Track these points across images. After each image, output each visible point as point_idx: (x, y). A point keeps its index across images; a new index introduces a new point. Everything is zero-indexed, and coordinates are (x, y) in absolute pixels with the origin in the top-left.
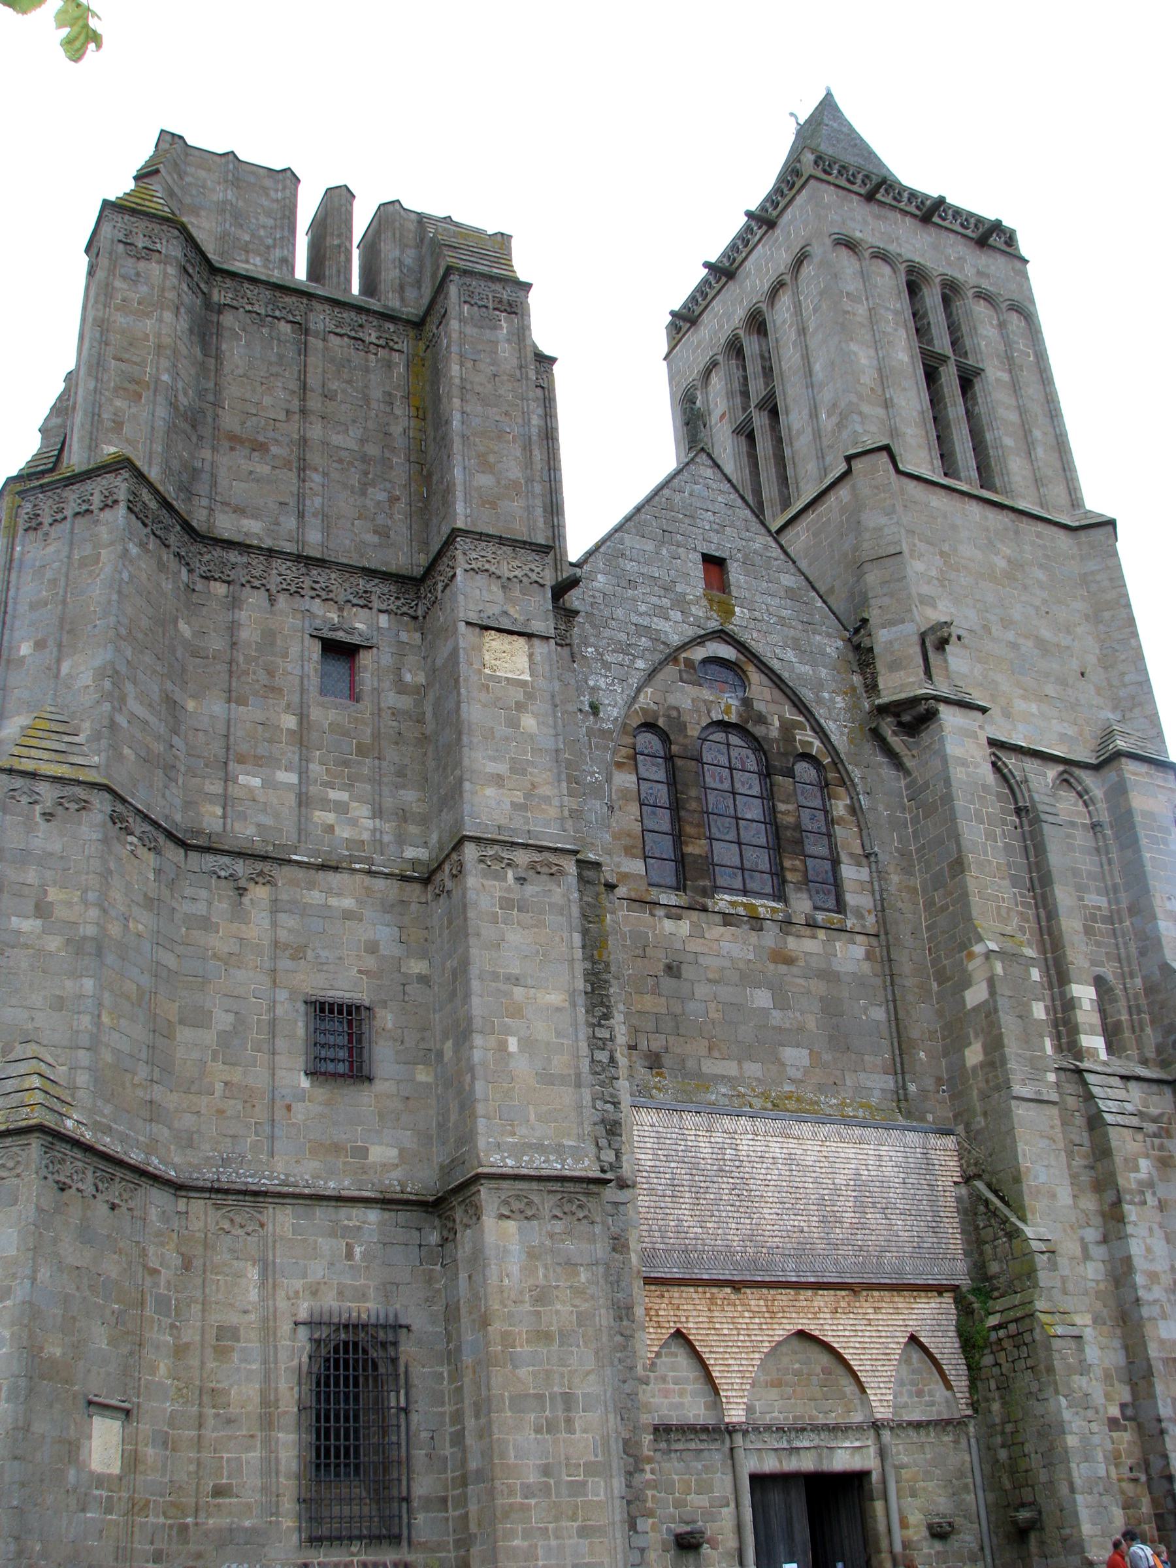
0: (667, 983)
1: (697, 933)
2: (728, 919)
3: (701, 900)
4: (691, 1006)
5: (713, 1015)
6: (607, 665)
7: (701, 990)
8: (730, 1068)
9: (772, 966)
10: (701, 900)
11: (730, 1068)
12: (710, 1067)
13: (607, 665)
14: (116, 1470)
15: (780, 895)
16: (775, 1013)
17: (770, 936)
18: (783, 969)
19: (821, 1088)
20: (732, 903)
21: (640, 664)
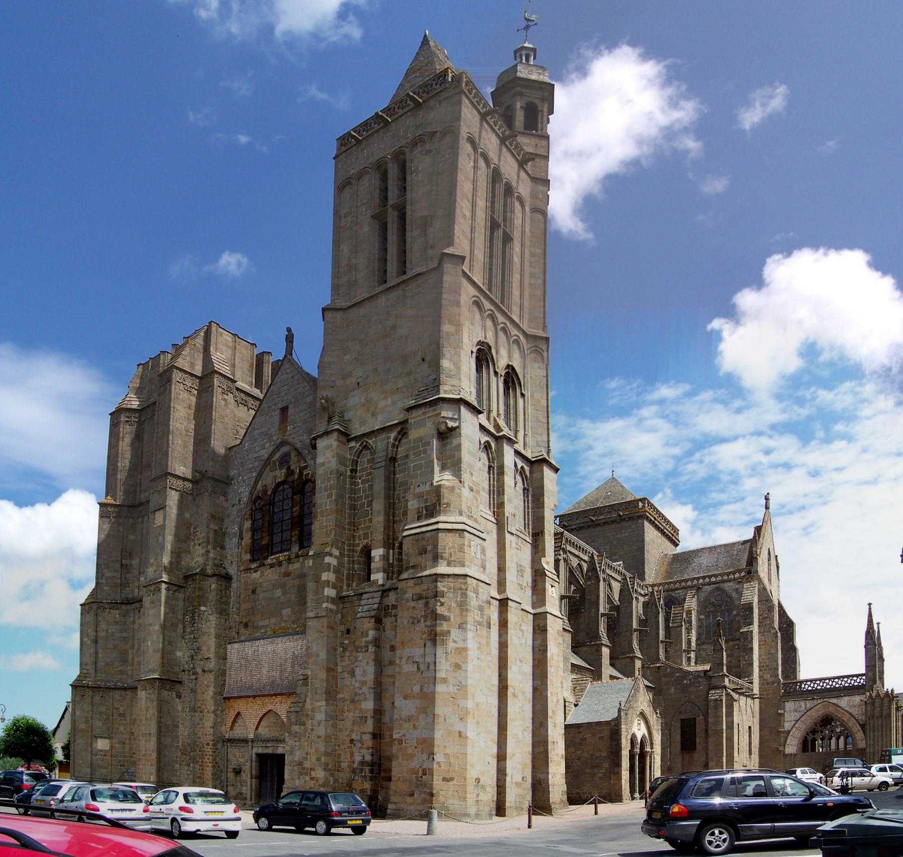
0: (252, 596)
1: (262, 575)
2: (272, 566)
4: (258, 602)
5: (264, 604)
6: (244, 481)
7: (261, 596)
8: (266, 622)
9: (283, 579)
11: (266, 622)
13: (244, 481)
15: (289, 550)
16: (282, 597)
17: (283, 569)
18: (286, 578)
19: (293, 622)
20: (272, 559)
21: (255, 474)
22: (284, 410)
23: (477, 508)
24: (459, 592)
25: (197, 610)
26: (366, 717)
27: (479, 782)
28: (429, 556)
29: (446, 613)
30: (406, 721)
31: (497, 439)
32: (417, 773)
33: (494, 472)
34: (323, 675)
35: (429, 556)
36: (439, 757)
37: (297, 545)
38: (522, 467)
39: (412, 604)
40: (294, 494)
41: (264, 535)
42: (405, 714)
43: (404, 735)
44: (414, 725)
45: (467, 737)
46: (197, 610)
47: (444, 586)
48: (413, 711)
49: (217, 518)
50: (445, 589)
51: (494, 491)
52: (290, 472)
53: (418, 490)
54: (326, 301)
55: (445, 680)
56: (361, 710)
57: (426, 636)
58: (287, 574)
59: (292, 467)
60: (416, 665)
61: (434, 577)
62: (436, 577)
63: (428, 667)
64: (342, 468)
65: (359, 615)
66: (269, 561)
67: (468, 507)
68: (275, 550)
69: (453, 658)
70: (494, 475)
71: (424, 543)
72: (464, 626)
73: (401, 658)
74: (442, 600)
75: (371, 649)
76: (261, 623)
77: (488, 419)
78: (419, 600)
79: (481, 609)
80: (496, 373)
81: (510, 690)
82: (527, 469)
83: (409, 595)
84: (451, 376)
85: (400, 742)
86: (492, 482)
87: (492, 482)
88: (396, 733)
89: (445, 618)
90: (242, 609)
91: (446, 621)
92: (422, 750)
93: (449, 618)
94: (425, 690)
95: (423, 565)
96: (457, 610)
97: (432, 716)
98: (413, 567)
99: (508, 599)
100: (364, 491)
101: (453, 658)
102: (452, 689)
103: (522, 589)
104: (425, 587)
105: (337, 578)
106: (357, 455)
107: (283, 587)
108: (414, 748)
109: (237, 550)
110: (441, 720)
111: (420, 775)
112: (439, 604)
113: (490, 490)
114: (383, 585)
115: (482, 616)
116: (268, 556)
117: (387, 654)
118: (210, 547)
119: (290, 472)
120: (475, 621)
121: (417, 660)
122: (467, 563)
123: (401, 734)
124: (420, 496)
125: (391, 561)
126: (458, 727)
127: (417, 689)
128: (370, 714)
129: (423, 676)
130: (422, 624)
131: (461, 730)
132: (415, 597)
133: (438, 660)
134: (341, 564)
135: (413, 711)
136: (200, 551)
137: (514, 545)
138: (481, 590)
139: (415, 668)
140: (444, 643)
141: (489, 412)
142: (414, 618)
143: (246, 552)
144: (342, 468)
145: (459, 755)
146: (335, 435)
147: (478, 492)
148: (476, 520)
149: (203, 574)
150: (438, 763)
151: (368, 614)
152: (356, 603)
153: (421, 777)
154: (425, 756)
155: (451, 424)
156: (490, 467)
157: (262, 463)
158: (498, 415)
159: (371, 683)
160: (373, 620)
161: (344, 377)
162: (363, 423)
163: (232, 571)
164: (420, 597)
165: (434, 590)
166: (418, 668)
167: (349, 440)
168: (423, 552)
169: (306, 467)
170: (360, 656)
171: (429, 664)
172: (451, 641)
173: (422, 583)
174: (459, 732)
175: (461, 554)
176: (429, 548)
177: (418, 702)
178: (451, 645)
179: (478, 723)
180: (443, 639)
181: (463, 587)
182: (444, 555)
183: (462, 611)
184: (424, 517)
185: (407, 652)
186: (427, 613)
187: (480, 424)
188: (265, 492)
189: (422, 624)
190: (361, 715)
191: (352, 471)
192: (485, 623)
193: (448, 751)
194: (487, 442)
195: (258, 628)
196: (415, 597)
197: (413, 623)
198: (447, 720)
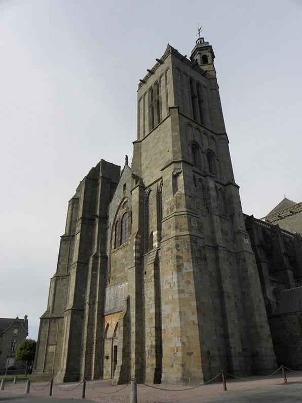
12: (118, 276)
14: (54, 350)
24: (186, 243)
27: (210, 354)
31: (204, 176)
32: (173, 350)
39: (166, 253)
43: (167, 327)
53: (167, 201)
54: (136, 139)
67: (189, 204)
73: (163, 282)
74: (178, 248)
78: (168, 250)
91: (180, 258)
93: (182, 257)
99: (217, 246)
102: (187, 295)
105: (140, 248)
115: (200, 255)
120: (196, 257)
124: (167, 204)
127: (170, 297)
130: (171, 263)
151: (151, 262)
159: (153, 298)
160: (153, 265)
166: (170, 286)
179: (204, 314)
188: (119, 218)
189: (171, 263)
192: (202, 258)
193: (188, 334)
195: (116, 278)
197: (167, 263)
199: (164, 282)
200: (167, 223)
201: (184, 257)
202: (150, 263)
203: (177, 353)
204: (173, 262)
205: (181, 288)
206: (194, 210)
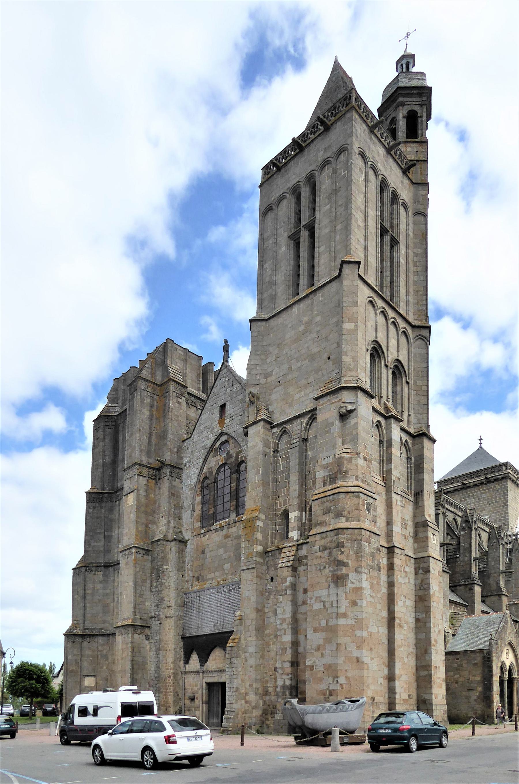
0: (202, 556)
2: (216, 530)
3: (209, 528)
8: (212, 575)
9: (224, 540)
10: (209, 528)
11: (212, 575)
16: (224, 555)
17: (224, 532)
18: (227, 540)
20: (216, 525)
22: (223, 407)
23: (370, 474)
24: (355, 542)
25: (161, 569)
26: (286, 648)
27: (374, 700)
28: (332, 515)
29: (345, 560)
30: (316, 651)
31: (386, 418)
32: (324, 694)
33: (383, 446)
34: (253, 615)
35: (332, 515)
36: (342, 680)
37: (235, 513)
38: (406, 441)
39: (319, 554)
40: (232, 473)
41: (210, 507)
42: (315, 644)
43: (314, 662)
44: (322, 654)
45: (363, 662)
46: (161, 569)
47: (344, 538)
48: (321, 642)
49: (174, 495)
50: (344, 540)
51: (383, 460)
52: (229, 456)
55: (344, 615)
56: (282, 642)
57: (330, 579)
58: (227, 537)
59: (231, 452)
60: (322, 603)
61: (336, 531)
62: (338, 531)
63: (332, 605)
64: (267, 450)
65: (280, 566)
66: (214, 527)
68: (218, 518)
69: (352, 597)
70: (383, 447)
71: (328, 504)
72: (360, 569)
73: (311, 598)
74: (342, 549)
75: (289, 592)
76: (209, 577)
77: (380, 403)
79: (373, 555)
80: (386, 366)
81: (397, 621)
82: (410, 441)
83: (317, 548)
84: (351, 369)
85: (312, 668)
86: (382, 454)
87: (382, 454)
88: (308, 661)
89: (345, 564)
90: (194, 566)
92: (328, 674)
93: (348, 563)
94: (330, 624)
95: (327, 522)
96: (354, 557)
97: (335, 645)
98: (320, 524)
100: (284, 467)
101: (352, 597)
102: (350, 622)
103: (406, 539)
104: (329, 539)
106: (278, 438)
107: (225, 547)
108: (322, 672)
109: (191, 520)
110: (343, 648)
111: (327, 696)
112: (340, 553)
113: (380, 460)
114: (298, 541)
116: (213, 523)
117: (301, 596)
118: (170, 518)
119: (229, 456)
120: (368, 565)
121: (324, 600)
122: (362, 519)
123: (312, 662)
125: (304, 521)
126: (356, 654)
127: (323, 623)
128: (289, 645)
129: (328, 612)
130: (327, 570)
131: (358, 656)
132: (321, 548)
133: (339, 599)
134: (266, 525)
135: (321, 642)
136: (163, 522)
137: (399, 503)
138: (373, 540)
139: (322, 607)
140: (344, 585)
141: (381, 397)
142: (320, 565)
143: (197, 522)
144: (267, 450)
145: (358, 678)
146: (262, 423)
147: (370, 461)
148: (369, 484)
149: (165, 539)
150: (341, 685)
152: (278, 556)
153: (328, 698)
154: (330, 680)
155: (350, 407)
156: (380, 441)
157: (207, 450)
158: (388, 399)
159: (289, 620)
160: (290, 569)
161: (266, 377)
162: (282, 412)
163: (187, 535)
164: (325, 548)
165: (336, 541)
167: (272, 428)
168: (327, 511)
169: (241, 451)
170: (280, 598)
171: (332, 602)
172: (349, 582)
173: (326, 537)
174: (357, 658)
175: (357, 511)
176: (332, 508)
177: (324, 634)
178: (349, 585)
179: (371, 650)
180: (343, 581)
181: (359, 538)
182: (344, 513)
183: (357, 557)
184: (328, 484)
185: (315, 594)
186: (331, 561)
187: (373, 407)
190: (282, 647)
191: (274, 452)
193: (349, 675)
194: (379, 421)
195: (207, 580)
196: (321, 548)
197: (320, 570)
198: (347, 648)
199: (314, 599)
200: (323, 503)
201: (350, 565)
202: (284, 565)
203: (331, 697)
204: (332, 569)
205: (342, 610)
206: (369, 484)
